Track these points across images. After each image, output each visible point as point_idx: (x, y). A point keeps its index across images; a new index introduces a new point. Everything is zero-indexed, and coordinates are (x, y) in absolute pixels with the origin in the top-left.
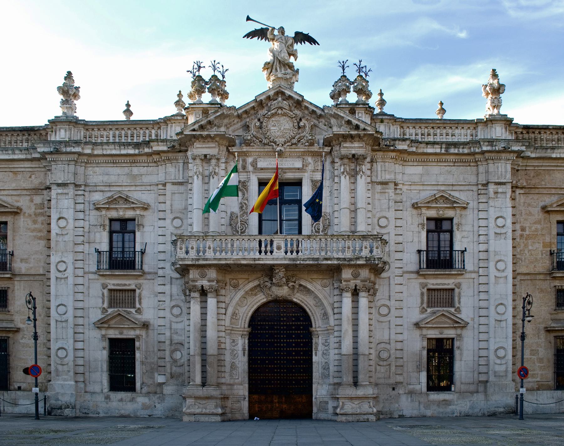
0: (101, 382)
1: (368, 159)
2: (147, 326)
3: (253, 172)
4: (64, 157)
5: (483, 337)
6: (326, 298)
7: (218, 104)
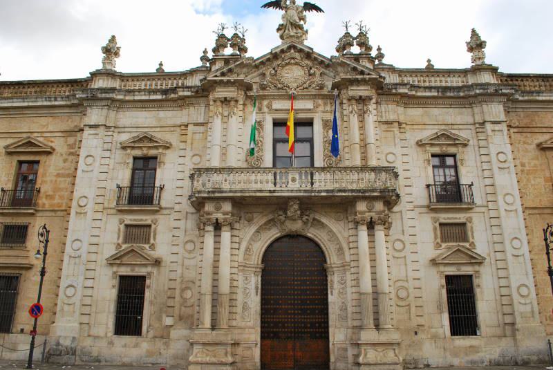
0: (107, 324)
1: (374, 101)
2: (160, 262)
3: (268, 113)
4: (99, 103)
5: (502, 273)
6: (340, 232)
7: (238, 55)
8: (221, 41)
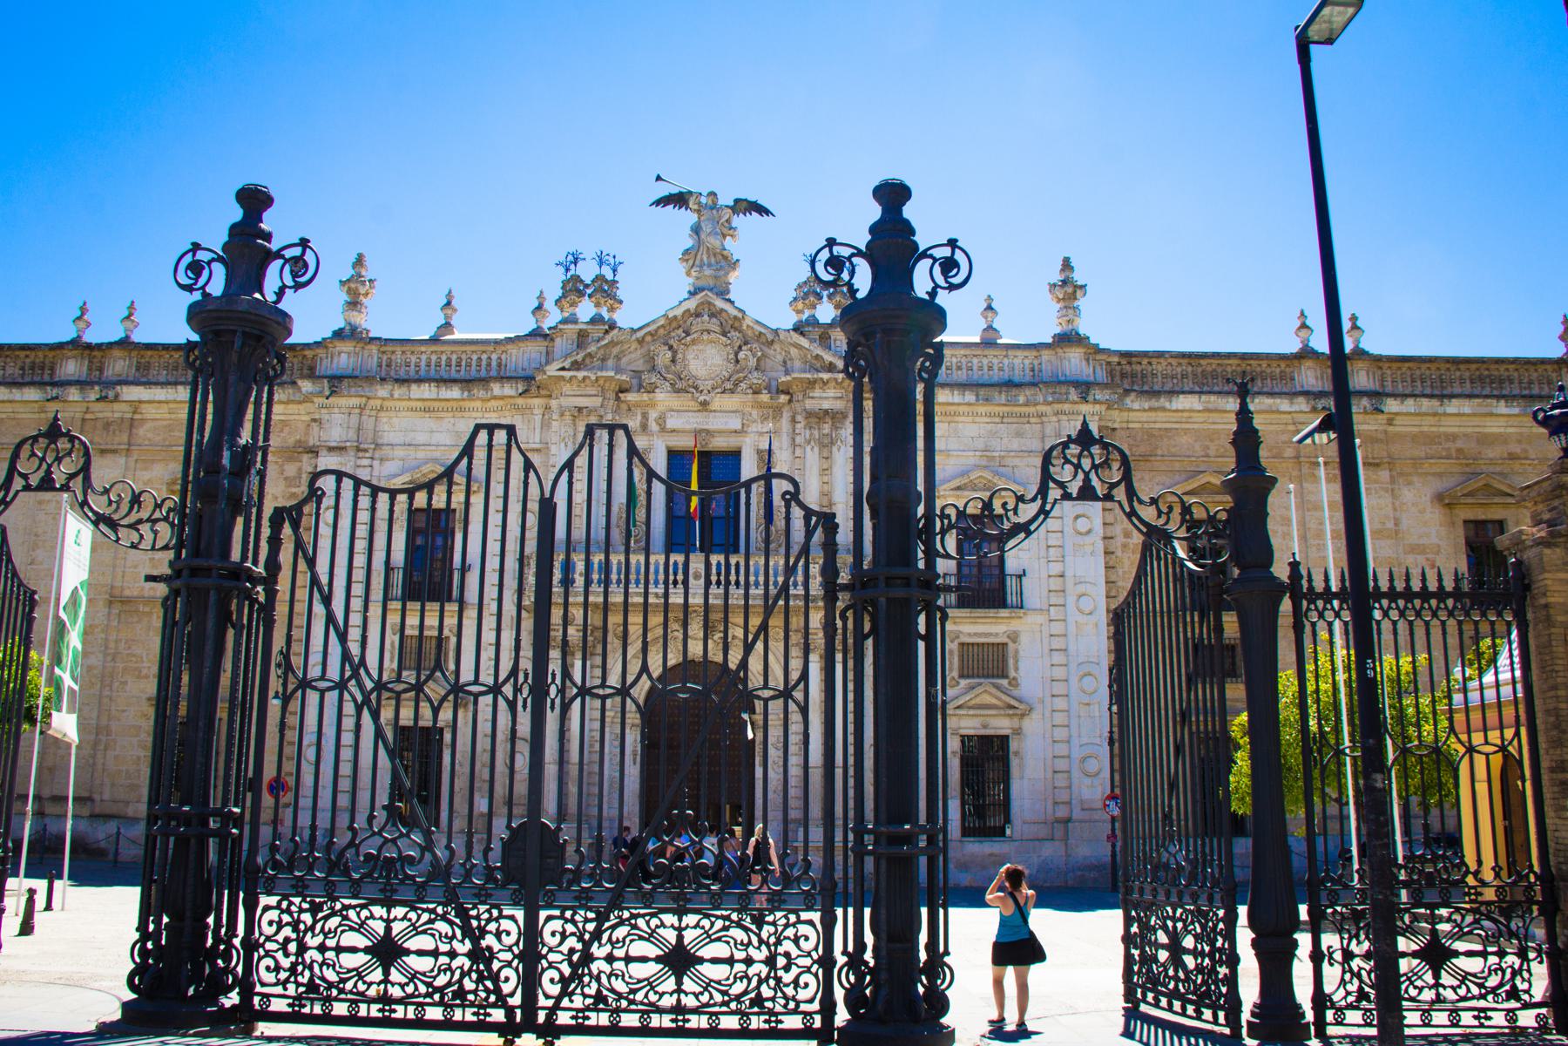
8: (573, 288)
